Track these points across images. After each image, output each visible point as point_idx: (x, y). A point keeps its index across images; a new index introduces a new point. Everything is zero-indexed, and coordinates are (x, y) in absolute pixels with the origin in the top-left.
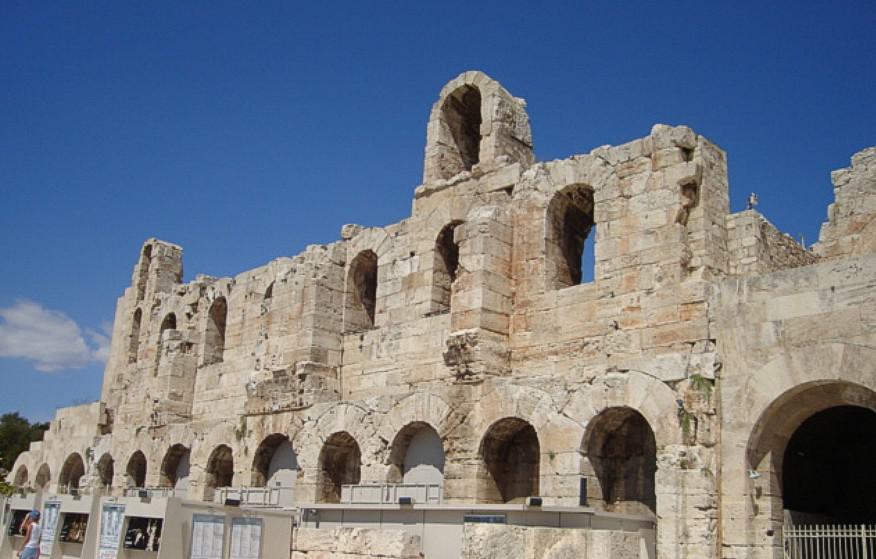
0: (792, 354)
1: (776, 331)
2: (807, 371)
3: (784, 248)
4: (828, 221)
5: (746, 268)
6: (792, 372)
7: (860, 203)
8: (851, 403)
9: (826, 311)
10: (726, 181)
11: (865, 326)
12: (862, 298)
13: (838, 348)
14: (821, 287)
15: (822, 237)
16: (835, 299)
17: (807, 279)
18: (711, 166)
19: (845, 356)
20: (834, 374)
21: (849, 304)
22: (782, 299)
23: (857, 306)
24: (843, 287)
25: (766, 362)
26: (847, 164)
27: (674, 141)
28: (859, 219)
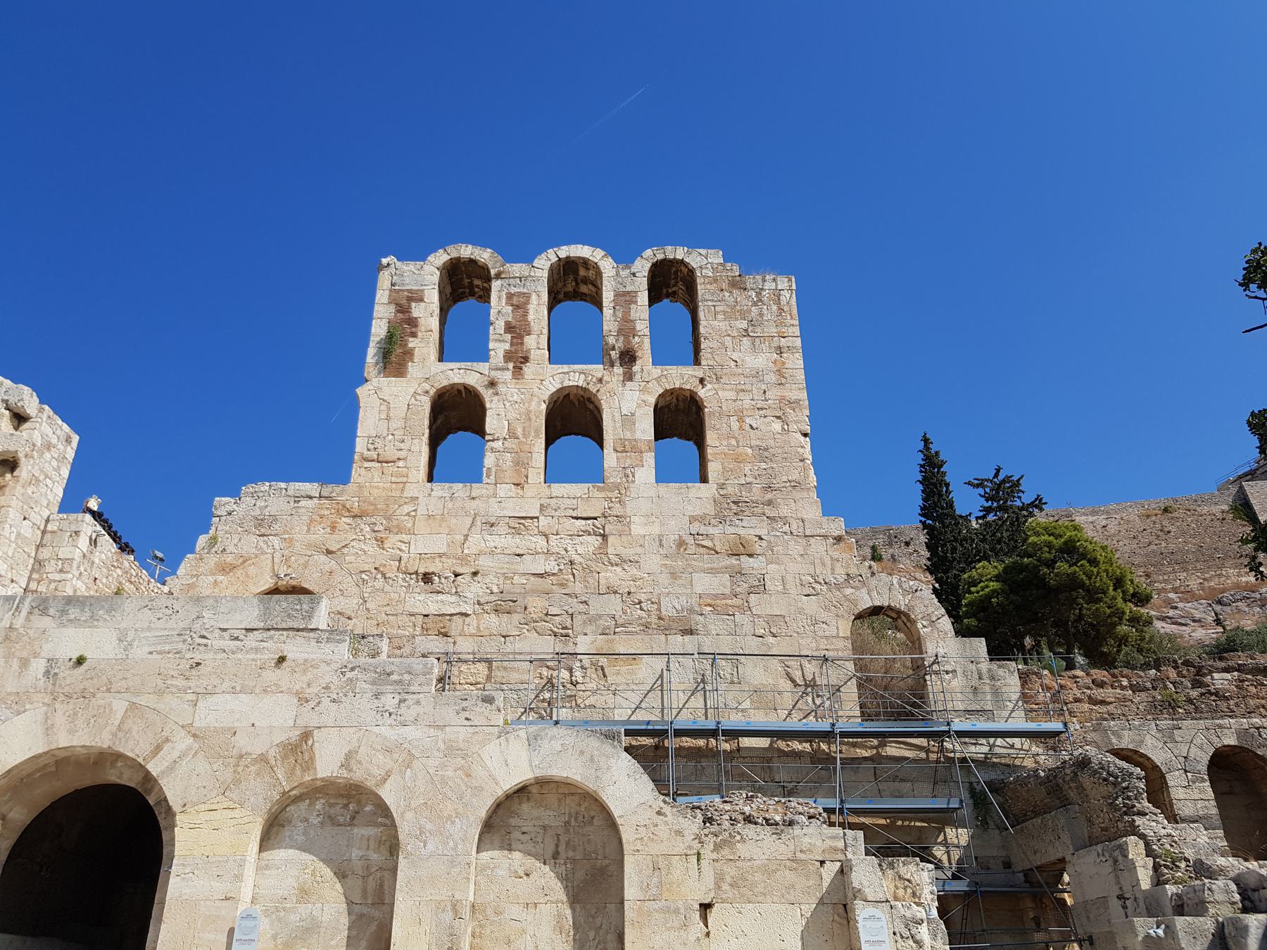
0: (57, 706)
1: (47, 673)
2: (72, 732)
3: (119, 571)
4: (193, 552)
5: (53, 586)
6: (49, 730)
7: (236, 541)
8: (119, 781)
9: (119, 656)
10: (65, 473)
11: (160, 682)
12: (167, 648)
13: (120, 706)
14: (123, 625)
15: (181, 571)
16: (136, 643)
17: (108, 612)
18: (49, 446)
19: (125, 717)
20: (103, 741)
21: (151, 653)
22: (70, 631)
23: (159, 657)
24: (149, 629)
25: (19, 713)
26: (235, 493)
27: (6, 402)
28: (229, 559)
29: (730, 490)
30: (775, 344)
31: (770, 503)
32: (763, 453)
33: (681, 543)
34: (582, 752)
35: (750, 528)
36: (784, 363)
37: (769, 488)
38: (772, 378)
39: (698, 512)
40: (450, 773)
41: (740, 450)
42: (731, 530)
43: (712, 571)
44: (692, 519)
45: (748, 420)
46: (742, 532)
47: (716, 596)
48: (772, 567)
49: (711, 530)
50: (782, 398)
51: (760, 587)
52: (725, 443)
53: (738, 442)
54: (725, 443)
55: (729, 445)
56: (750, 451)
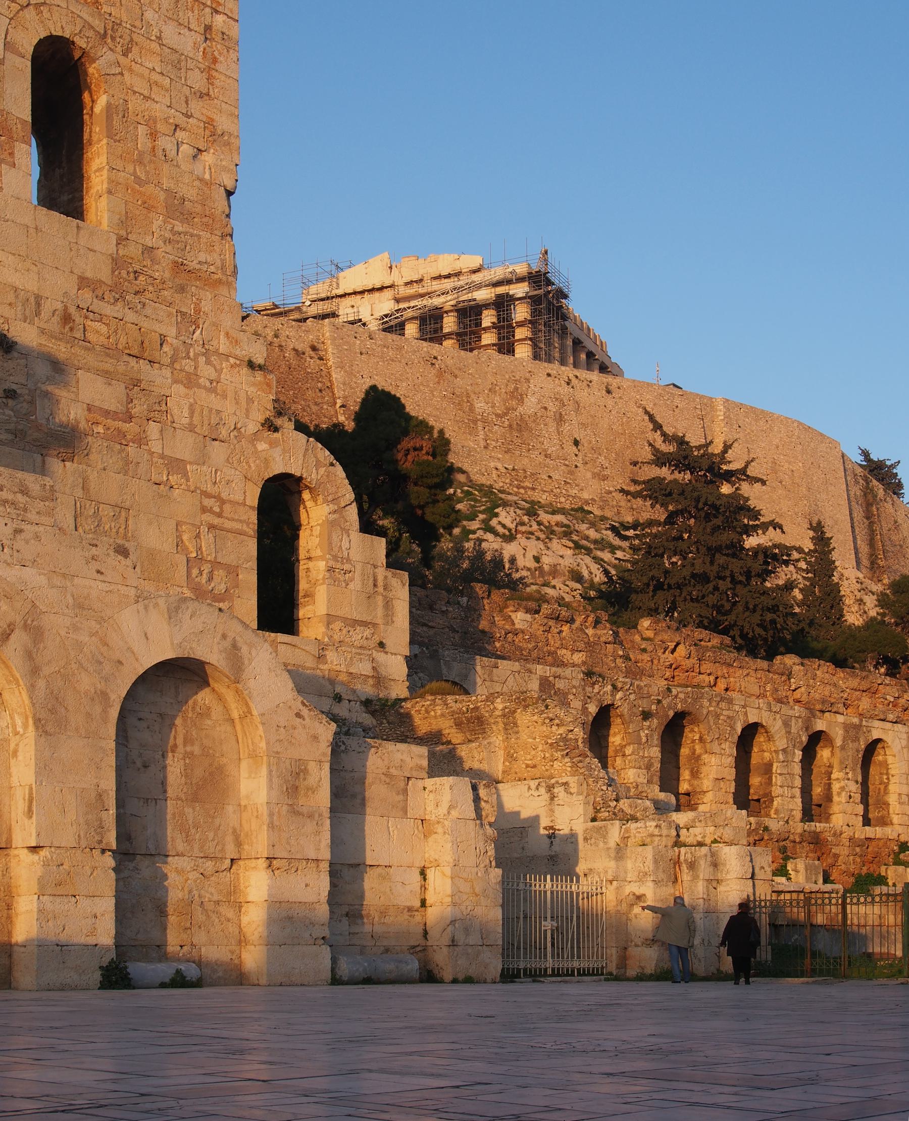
29: (132, 250)
30: (208, 21)
31: (182, 289)
32: (177, 207)
33: (67, 318)
34: (224, 637)
35: (160, 322)
36: (215, 61)
37: (178, 267)
38: (197, 80)
39: (89, 274)
40: (84, 638)
41: (150, 189)
42: (131, 316)
43: (108, 376)
44: (83, 282)
45: (166, 143)
46: (145, 324)
47: (107, 413)
48: (181, 389)
49: (108, 310)
50: (209, 123)
51: (159, 409)
52: (130, 168)
53: (147, 173)
54: (130, 168)
55: (134, 174)
56: (162, 196)
